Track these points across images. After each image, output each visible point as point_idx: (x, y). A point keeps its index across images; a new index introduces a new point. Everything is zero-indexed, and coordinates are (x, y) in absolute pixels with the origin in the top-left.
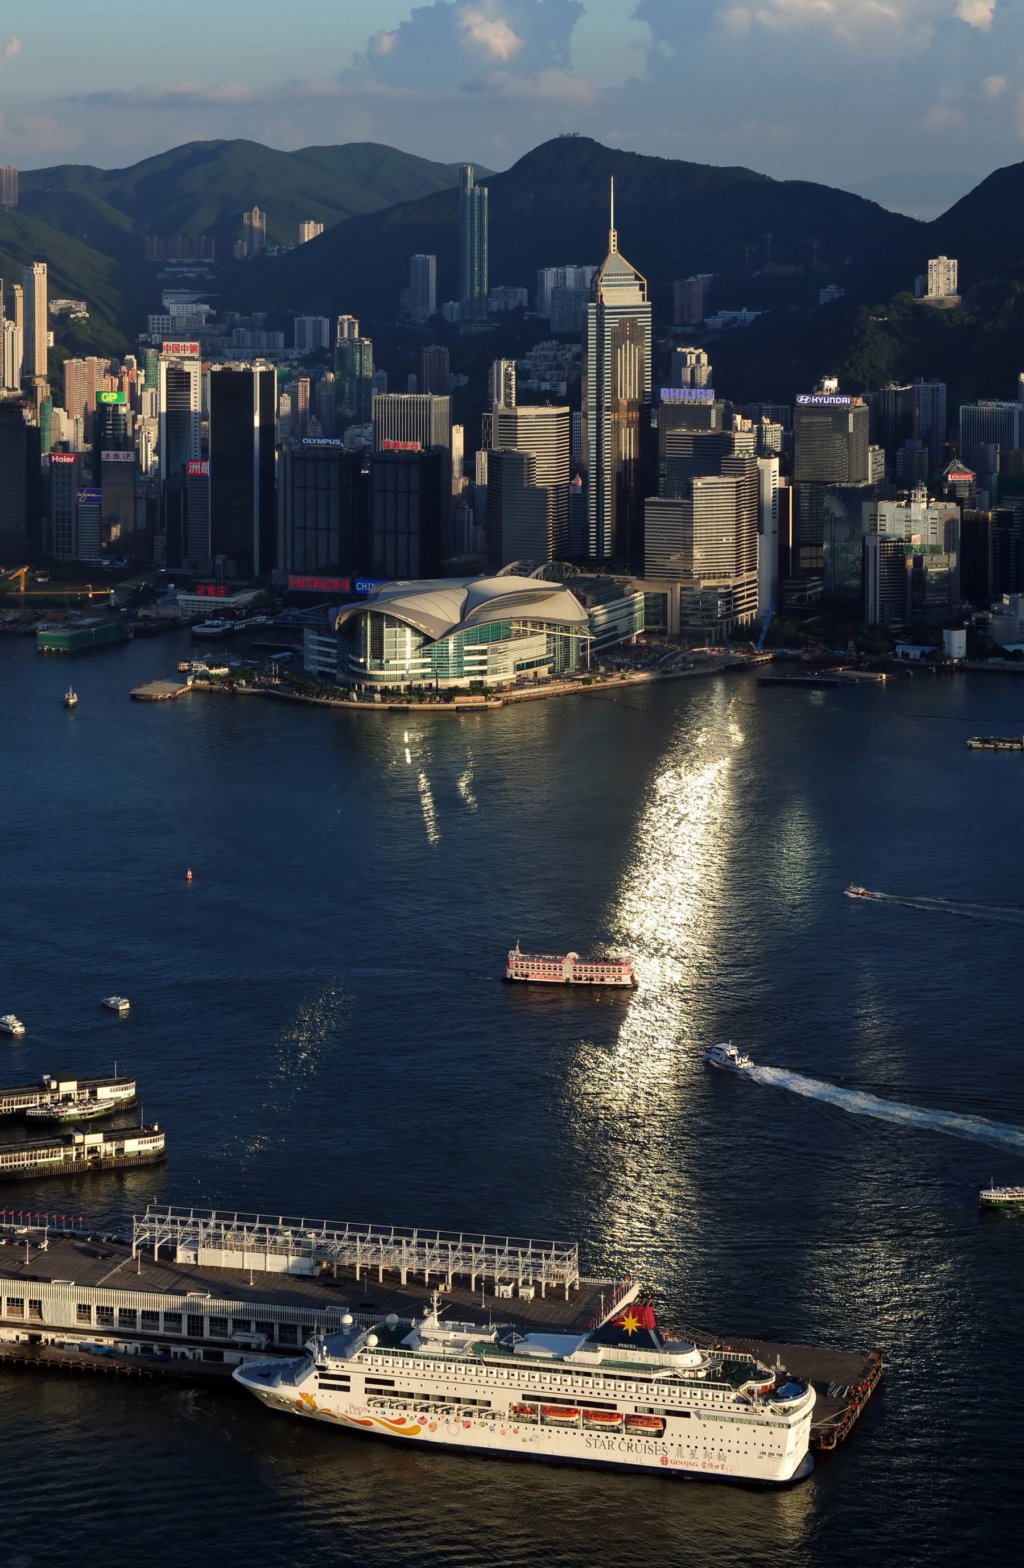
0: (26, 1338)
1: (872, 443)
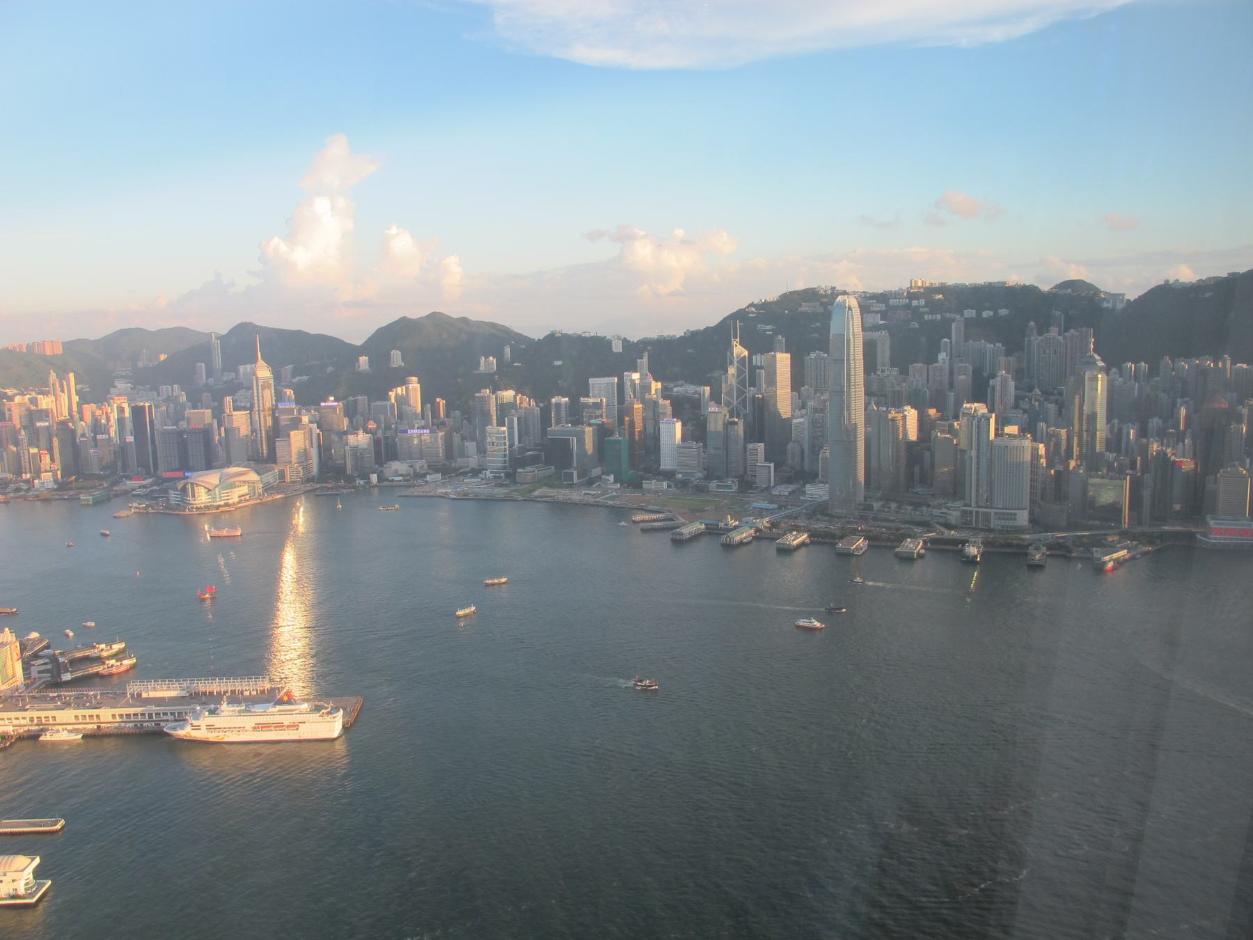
0: (96, 727)
1: (345, 417)
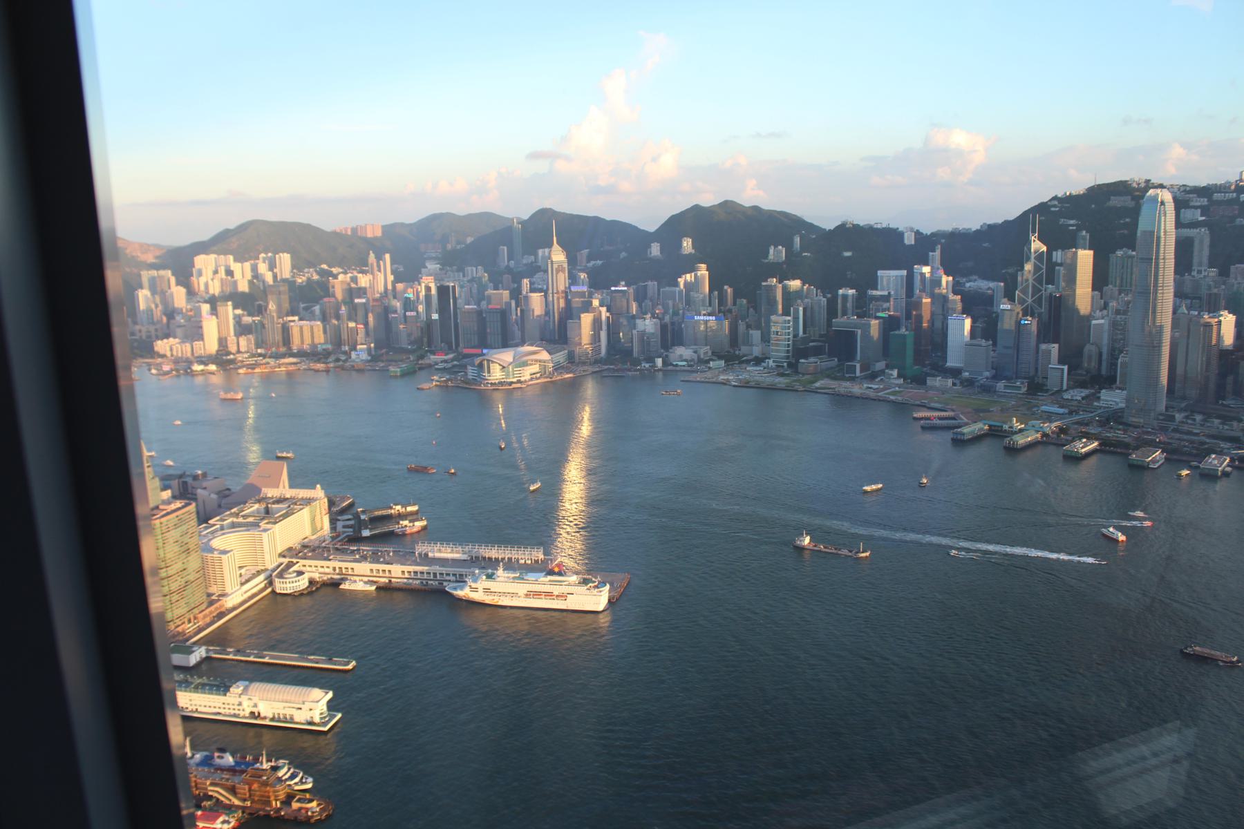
0: (387, 581)
